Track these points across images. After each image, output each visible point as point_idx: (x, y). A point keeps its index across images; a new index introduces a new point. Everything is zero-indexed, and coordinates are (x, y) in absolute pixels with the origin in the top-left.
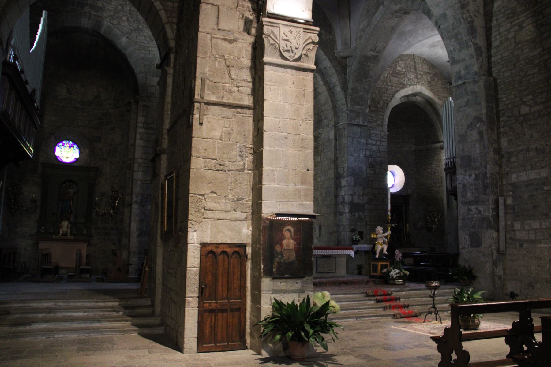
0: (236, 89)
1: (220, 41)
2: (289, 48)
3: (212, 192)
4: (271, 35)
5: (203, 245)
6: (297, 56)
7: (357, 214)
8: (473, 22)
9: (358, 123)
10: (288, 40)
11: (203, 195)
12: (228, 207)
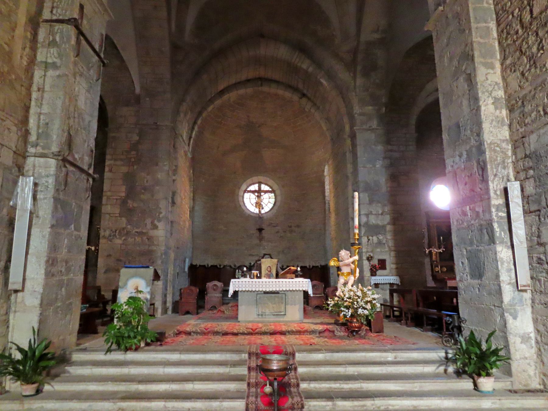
7: (375, 238)
9: (370, 127)
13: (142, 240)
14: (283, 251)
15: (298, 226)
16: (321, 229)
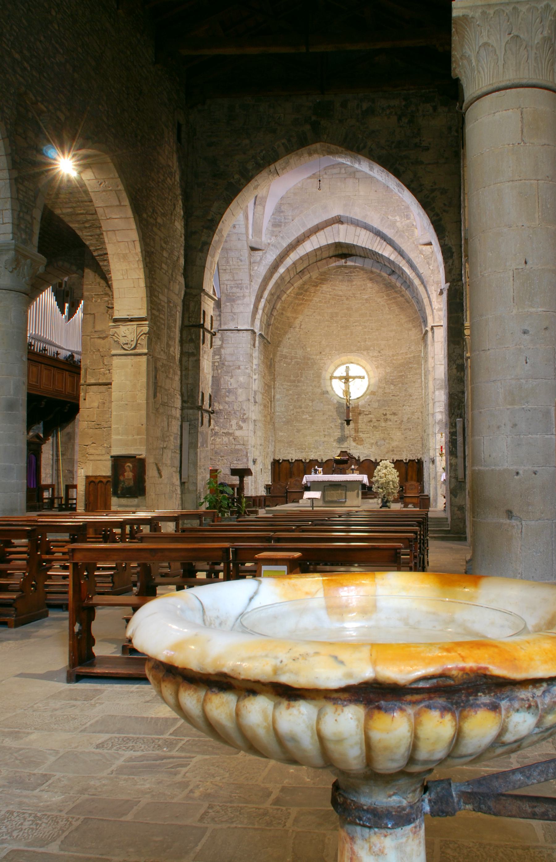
0: (108, 372)
1: (96, 340)
2: (127, 342)
3: (93, 443)
4: (115, 335)
5: (87, 477)
6: (133, 346)
8: (440, 220)
10: (125, 336)
11: (87, 446)
12: (104, 452)
13: (229, 440)
14: (377, 442)
15: (394, 414)
16: (418, 418)
